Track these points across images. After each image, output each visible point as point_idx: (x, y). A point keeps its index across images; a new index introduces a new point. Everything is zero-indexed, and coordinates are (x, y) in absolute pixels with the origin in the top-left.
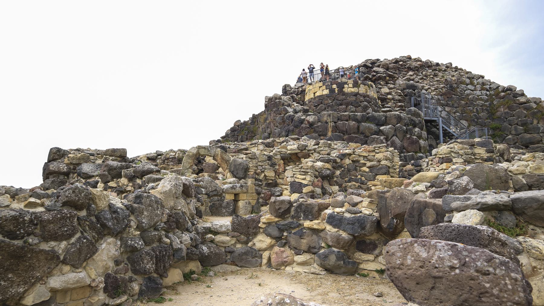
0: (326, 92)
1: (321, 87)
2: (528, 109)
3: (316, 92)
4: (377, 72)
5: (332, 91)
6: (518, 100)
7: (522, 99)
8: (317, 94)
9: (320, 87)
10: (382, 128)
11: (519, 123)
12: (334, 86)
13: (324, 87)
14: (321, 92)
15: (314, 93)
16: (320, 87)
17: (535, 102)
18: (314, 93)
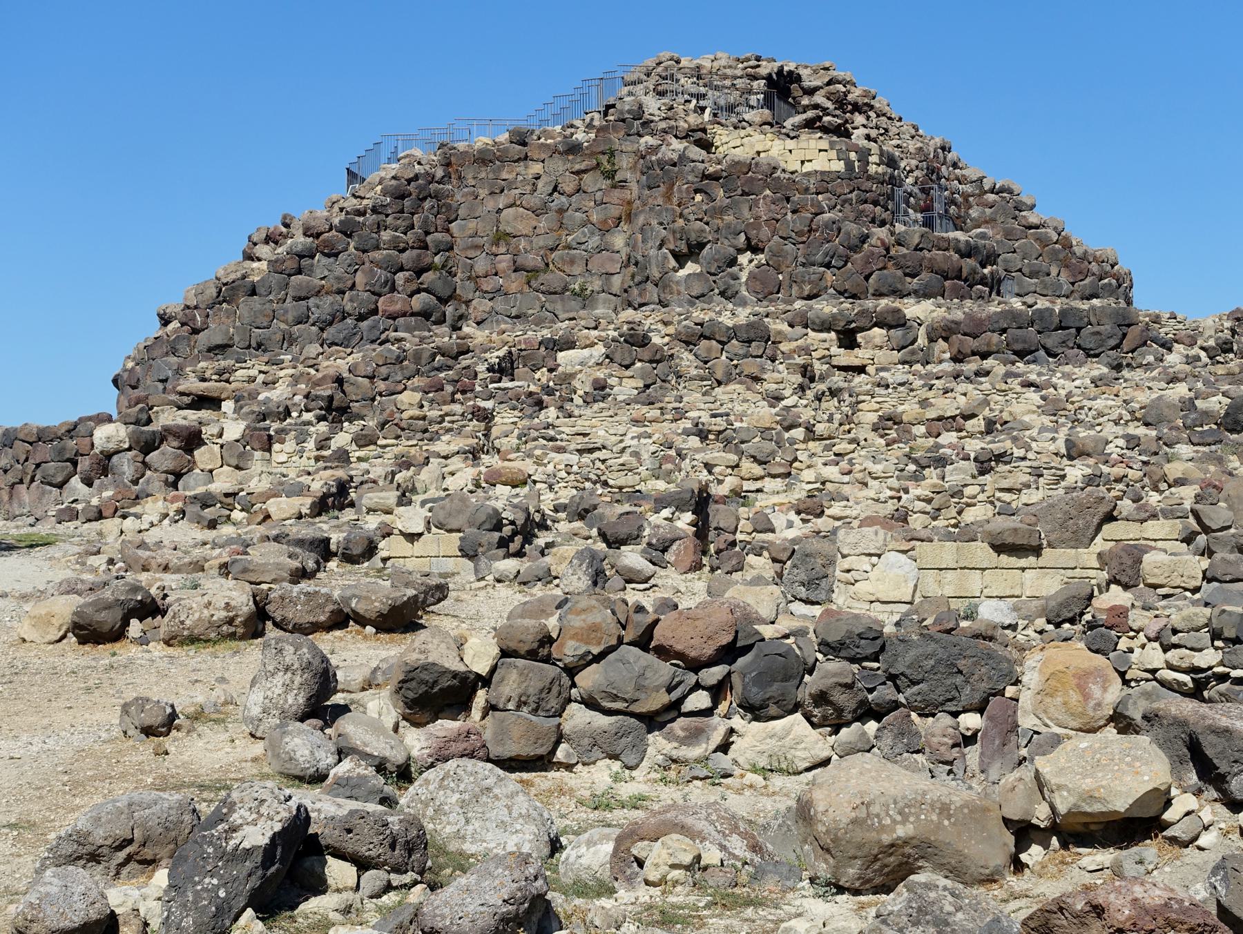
0: (839, 166)
1: (826, 151)
2: (1044, 242)
3: (811, 161)
4: (824, 109)
5: (849, 165)
6: (1025, 217)
7: (1033, 218)
8: (808, 167)
9: (820, 151)
10: (986, 271)
11: (1026, 270)
12: (853, 156)
13: (833, 154)
14: (827, 163)
15: (803, 162)
16: (820, 151)
17: (1055, 229)
18: (803, 162)
